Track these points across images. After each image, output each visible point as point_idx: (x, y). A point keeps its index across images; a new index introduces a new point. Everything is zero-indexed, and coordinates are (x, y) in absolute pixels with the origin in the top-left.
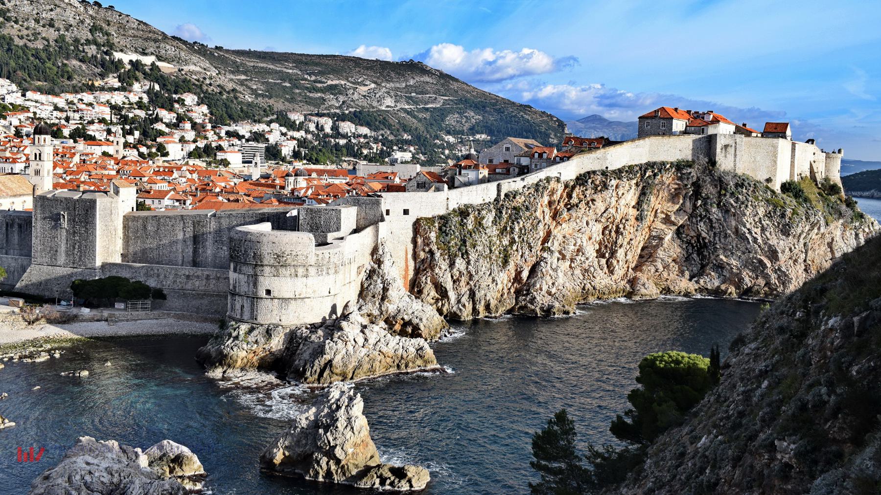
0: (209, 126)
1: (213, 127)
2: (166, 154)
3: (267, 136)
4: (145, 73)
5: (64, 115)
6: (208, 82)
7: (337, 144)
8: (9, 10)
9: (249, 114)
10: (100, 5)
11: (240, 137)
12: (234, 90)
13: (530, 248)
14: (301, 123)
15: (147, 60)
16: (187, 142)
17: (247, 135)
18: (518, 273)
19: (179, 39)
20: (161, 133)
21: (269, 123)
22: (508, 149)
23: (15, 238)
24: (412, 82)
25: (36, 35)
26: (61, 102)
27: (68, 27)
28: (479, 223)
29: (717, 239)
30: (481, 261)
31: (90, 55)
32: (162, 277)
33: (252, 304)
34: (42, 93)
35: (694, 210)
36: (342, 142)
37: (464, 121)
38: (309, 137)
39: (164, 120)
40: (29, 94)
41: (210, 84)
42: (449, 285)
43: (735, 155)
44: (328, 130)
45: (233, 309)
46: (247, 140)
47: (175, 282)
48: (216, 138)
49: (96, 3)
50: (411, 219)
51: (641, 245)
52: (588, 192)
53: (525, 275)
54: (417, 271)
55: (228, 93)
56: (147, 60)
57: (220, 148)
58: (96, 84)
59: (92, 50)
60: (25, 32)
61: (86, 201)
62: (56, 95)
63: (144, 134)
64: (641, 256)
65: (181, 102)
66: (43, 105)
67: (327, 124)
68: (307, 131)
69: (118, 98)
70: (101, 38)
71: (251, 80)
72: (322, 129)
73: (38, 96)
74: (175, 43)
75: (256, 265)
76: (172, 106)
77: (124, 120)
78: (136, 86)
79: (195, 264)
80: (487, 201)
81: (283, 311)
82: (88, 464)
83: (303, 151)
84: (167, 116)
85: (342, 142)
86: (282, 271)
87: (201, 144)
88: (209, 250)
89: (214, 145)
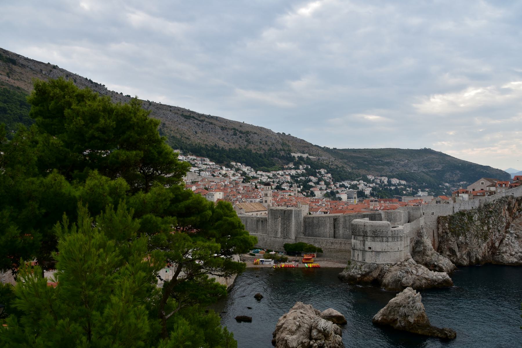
1: (334, 183)
2: (315, 196)
3: (358, 186)
4: (304, 162)
5: (272, 180)
6: (331, 164)
12: (343, 167)
13: (499, 231)
14: (373, 180)
15: (305, 156)
16: (322, 190)
17: (349, 186)
18: (493, 244)
19: (318, 146)
21: (358, 181)
22: (482, 183)
23: (260, 227)
24: (426, 158)
25: (260, 148)
26: (271, 175)
27: (273, 144)
28: (470, 218)
30: (473, 238)
32: (321, 243)
33: (363, 254)
36: (393, 188)
37: (454, 176)
38: (377, 186)
41: (332, 165)
42: (456, 249)
44: (386, 183)
45: (354, 256)
46: (349, 189)
47: (326, 245)
48: (335, 188)
50: (435, 218)
53: (497, 245)
54: (440, 242)
57: (338, 192)
58: (284, 167)
59: (282, 153)
60: (256, 147)
61: (289, 210)
62: (269, 171)
63: (304, 187)
65: (320, 173)
66: (264, 176)
67: (385, 180)
68: (376, 184)
69: (293, 172)
72: (383, 182)
75: (364, 236)
78: (301, 167)
79: (335, 237)
80: (474, 208)
82: (301, 313)
85: (393, 188)
86: (377, 239)
88: (341, 231)
89: (335, 191)
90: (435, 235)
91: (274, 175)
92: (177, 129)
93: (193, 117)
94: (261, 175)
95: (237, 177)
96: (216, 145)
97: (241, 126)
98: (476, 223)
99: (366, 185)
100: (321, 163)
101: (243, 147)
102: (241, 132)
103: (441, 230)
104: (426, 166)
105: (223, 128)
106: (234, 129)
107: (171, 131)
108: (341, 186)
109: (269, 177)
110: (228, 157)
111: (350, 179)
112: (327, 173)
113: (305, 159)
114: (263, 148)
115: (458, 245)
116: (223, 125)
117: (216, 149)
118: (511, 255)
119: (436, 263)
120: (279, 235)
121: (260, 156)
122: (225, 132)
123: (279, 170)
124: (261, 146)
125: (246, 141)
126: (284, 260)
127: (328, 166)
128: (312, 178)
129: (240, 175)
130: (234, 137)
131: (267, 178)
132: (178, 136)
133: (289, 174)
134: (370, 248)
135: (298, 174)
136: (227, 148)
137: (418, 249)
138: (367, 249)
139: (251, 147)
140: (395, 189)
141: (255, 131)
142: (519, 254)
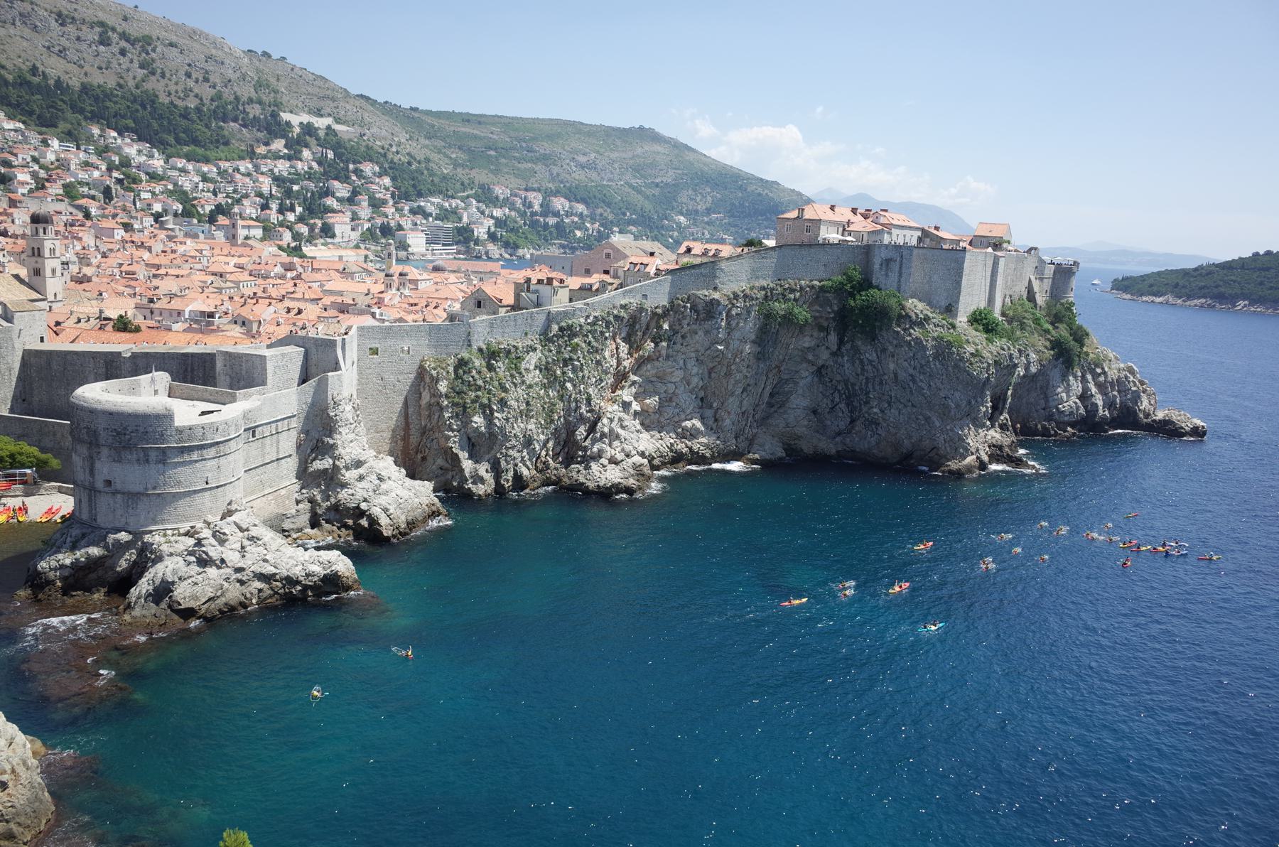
0: (391, 202)
2: (333, 236)
5: (211, 187)
6: (394, 149)
7: (546, 224)
8: (153, 60)
9: (443, 188)
10: (270, 56)
11: (426, 215)
12: (428, 160)
15: (321, 123)
19: (367, 99)
20: (334, 211)
22: (608, 256)
24: (639, 151)
25: (188, 91)
29: (870, 385)
31: (251, 116)
33: (90, 500)
34: (189, 161)
35: (839, 349)
38: (513, 213)
39: (338, 195)
40: (173, 160)
41: (398, 153)
43: (900, 274)
44: (537, 208)
48: (397, 216)
49: (265, 54)
51: (768, 390)
52: (685, 322)
54: (424, 431)
55: (419, 162)
57: (400, 228)
59: (254, 111)
60: (172, 88)
62: (207, 161)
64: (770, 405)
65: (358, 172)
67: (536, 200)
69: (282, 167)
71: (450, 147)
72: (530, 206)
73: (181, 163)
74: (357, 103)
76: (348, 177)
77: (288, 193)
78: (306, 153)
81: (130, 510)
84: (342, 190)
85: (552, 221)
87: (379, 221)
89: (393, 224)
90: (411, 410)
91: (222, 173)
94: (183, 171)
95: (96, 174)
97: (125, 19)
98: (529, 379)
99: (483, 213)
100: (367, 146)
101: (131, 84)
102: (124, 36)
104: (637, 170)
105: (62, 18)
106: (102, 24)
108: (414, 212)
109: (205, 179)
111: (440, 192)
112: (380, 176)
113: (322, 134)
114: (196, 91)
115: (469, 439)
117: (36, 80)
118: (613, 461)
119: (364, 506)
121: (185, 115)
122: (70, 28)
124: (191, 83)
125: (142, 67)
127: (385, 155)
128: (336, 184)
129: (104, 168)
130: (101, 47)
131: (197, 179)
133: (271, 170)
134: (108, 483)
136: (75, 83)
137: (319, 465)
138: (100, 485)
139: (154, 85)
140: (557, 226)
141: (174, 39)
142: (637, 459)
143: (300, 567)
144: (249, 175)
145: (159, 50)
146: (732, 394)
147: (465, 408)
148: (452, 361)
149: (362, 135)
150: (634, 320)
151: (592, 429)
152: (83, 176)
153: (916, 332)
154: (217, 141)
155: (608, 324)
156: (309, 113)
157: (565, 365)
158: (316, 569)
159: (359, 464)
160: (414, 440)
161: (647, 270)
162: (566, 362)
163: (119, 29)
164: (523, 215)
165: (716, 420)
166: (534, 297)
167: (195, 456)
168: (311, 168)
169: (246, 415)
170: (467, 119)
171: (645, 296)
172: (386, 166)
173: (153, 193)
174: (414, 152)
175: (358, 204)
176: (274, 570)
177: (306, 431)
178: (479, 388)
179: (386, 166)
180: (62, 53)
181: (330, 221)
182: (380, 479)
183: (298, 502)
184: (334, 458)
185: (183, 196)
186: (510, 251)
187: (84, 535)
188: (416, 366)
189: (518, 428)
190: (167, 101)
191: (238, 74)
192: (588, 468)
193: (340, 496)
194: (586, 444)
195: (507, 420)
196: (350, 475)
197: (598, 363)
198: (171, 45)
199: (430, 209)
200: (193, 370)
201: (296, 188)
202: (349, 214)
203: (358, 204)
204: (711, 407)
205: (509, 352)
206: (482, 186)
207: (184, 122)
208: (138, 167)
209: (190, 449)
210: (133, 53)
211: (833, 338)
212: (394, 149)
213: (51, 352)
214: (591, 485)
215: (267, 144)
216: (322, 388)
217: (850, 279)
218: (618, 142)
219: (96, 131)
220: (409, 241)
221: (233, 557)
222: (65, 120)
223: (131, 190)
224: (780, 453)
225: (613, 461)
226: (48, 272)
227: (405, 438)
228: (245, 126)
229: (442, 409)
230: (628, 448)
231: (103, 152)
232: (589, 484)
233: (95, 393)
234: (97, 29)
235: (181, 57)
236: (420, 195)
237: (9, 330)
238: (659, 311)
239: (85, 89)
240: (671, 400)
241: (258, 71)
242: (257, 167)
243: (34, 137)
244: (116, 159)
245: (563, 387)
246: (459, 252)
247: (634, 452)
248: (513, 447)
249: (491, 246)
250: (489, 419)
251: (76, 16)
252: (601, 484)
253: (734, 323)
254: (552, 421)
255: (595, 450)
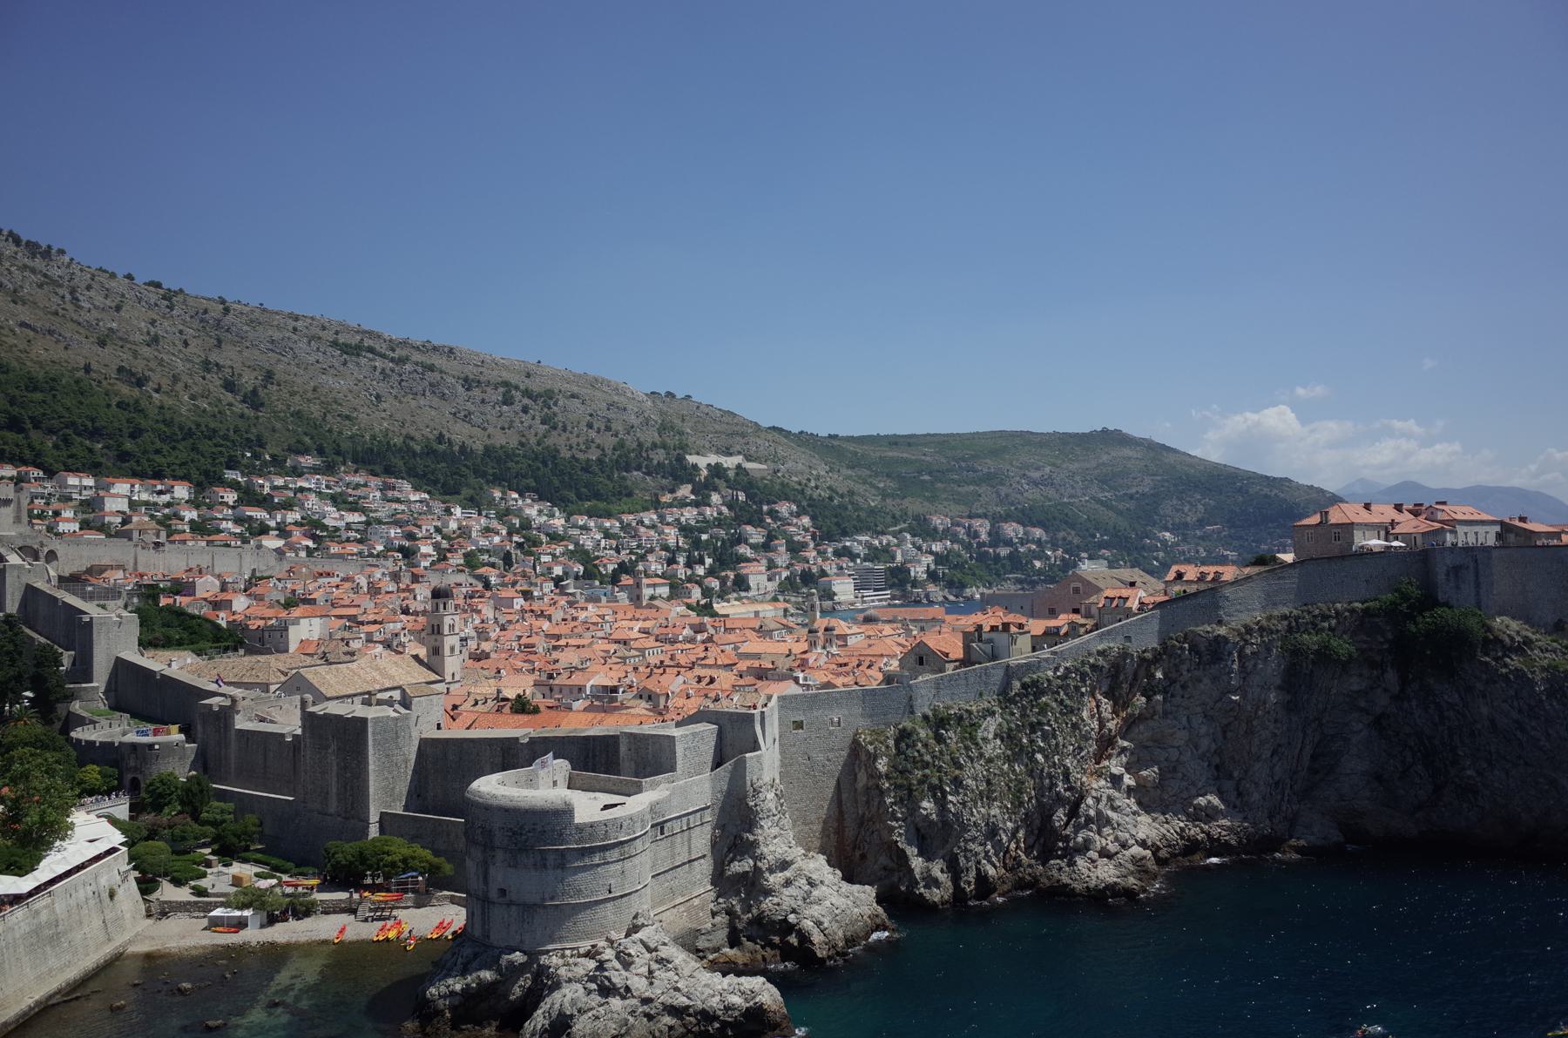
0: (812, 545)
2: (748, 589)
5: (614, 543)
6: (813, 484)
7: (997, 556)
9: (870, 523)
11: (853, 557)
12: (851, 493)
14: (947, 530)
15: (730, 462)
19: (779, 430)
20: (748, 560)
22: (1076, 590)
24: (1105, 458)
25: (589, 443)
33: (483, 913)
36: (1004, 552)
37: (1186, 509)
38: (956, 547)
43: (1478, 585)
44: (984, 537)
49: (669, 394)
51: (1308, 751)
52: (1184, 667)
54: (861, 822)
55: (842, 496)
56: (730, 462)
57: (823, 573)
59: (659, 456)
60: (574, 441)
62: (609, 516)
65: (773, 514)
67: (983, 528)
69: (689, 515)
70: (671, 441)
71: (877, 475)
72: (976, 535)
74: (770, 437)
76: (762, 521)
77: (697, 544)
78: (715, 498)
83: (941, 570)
84: (756, 535)
87: (799, 568)
89: (815, 570)
90: (844, 796)
91: (625, 527)
92: (314, 390)
93: (371, 350)
94: (585, 528)
95: (497, 539)
96: (441, 435)
99: (919, 548)
100: (782, 484)
101: (533, 441)
102: (527, 393)
103: (862, 779)
104: (1104, 481)
105: (468, 383)
106: (506, 384)
107: (293, 394)
108: (838, 554)
110: (478, 473)
111: (869, 529)
112: (798, 515)
113: (731, 474)
115: (918, 830)
116: (470, 371)
118: (1105, 854)
119: (792, 918)
120: (333, 807)
121: (586, 469)
122: (476, 392)
123: (646, 509)
124: (592, 434)
125: (543, 422)
126: (300, 910)
128: (749, 528)
129: (504, 532)
132: (315, 411)
133: (678, 520)
134: (503, 892)
135: (705, 521)
136: (478, 447)
138: (493, 894)
139: (555, 439)
140: (1011, 556)
141: (575, 389)
142: (1136, 850)
143: (717, 998)
144: (653, 527)
145: (560, 403)
146: (1258, 759)
147: (910, 791)
148: (891, 732)
149: (776, 472)
150: (1116, 668)
151: (1073, 812)
152: (483, 542)
153: (1515, 662)
154: (620, 493)
155: (1083, 676)
156: (717, 452)
157: (1033, 731)
158: (736, 1000)
159: (784, 865)
160: (850, 833)
161: (1128, 604)
162: (1034, 727)
163: (522, 387)
164: (968, 547)
165: (1239, 795)
166: (988, 648)
167: (597, 860)
168: (720, 513)
169: (653, 808)
170: (894, 441)
171: (1128, 638)
172: (805, 503)
173: (554, 555)
174: (835, 485)
175: (775, 550)
176: (686, 1002)
177: (721, 825)
178: (926, 765)
179: (805, 503)
180: (467, 418)
181: (744, 571)
182: (811, 883)
183: (714, 914)
184: (756, 859)
185: (581, 554)
186: (954, 591)
187: (476, 955)
188: (849, 741)
189: (978, 813)
190: (568, 455)
191: (641, 419)
192: (1072, 864)
193: (764, 906)
194: (1067, 832)
195: (964, 804)
196: (774, 879)
197: (1075, 726)
198: (573, 396)
199: (859, 549)
200: (594, 756)
201: (704, 537)
202: (764, 562)
203: (775, 550)
204: (1231, 777)
205: (960, 718)
206: (916, 518)
207: (585, 476)
208: (539, 529)
209: (591, 851)
210: (536, 409)
211: (1391, 676)
212: (813, 484)
213: (447, 741)
214: (1078, 886)
215: (672, 491)
216: (739, 772)
217: (1405, 597)
218: (1078, 450)
219: (497, 494)
220: (834, 589)
221: (639, 984)
222: (468, 485)
223: (531, 554)
224: (1336, 836)
225: (1105, 854)
226: (447, 651)
227: (840, 831)
228: (648, 474)
229: (882, 793)
230: (1123, 836)
231: (503, 516)
232: (1075, 885)
233: (491, 786)
234: (501, 390)
235: (582, 408)
236: (845, 533)
237: (406, 717)
238: (1148, 655)
239: (488, 451)
240: (1175, 770)
241: (662, 413)
242: (662, 518)
243: (438, 507)
244: (517, 522)
245: (1032, 759)
246: (893, 598)
247: (1131, 842)
248: (974, 839)
249: (931, 588)
250: (942, 804)
251: (482, 378)
252: (1093, 884)
253: (1249, 665)
254: (1021, 804)
255: (1080, 839)
